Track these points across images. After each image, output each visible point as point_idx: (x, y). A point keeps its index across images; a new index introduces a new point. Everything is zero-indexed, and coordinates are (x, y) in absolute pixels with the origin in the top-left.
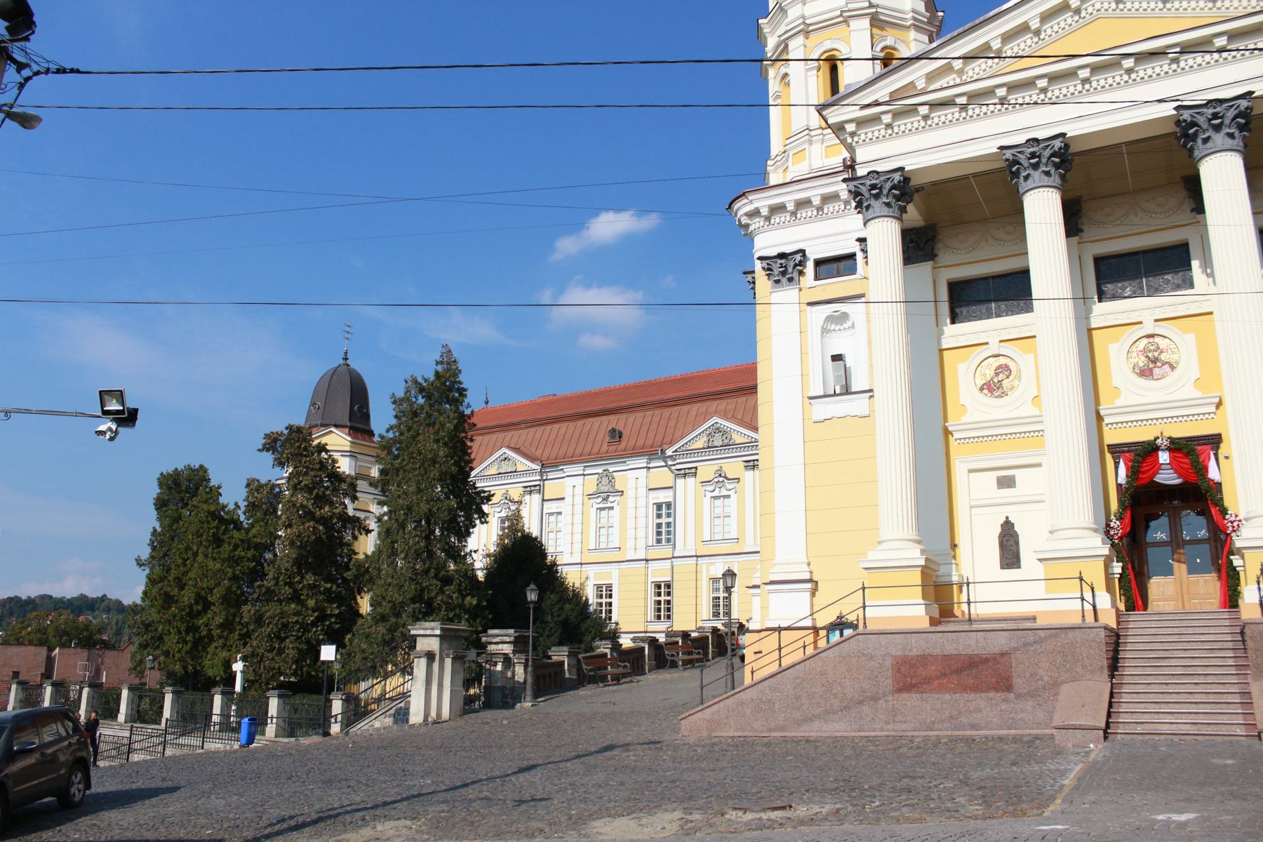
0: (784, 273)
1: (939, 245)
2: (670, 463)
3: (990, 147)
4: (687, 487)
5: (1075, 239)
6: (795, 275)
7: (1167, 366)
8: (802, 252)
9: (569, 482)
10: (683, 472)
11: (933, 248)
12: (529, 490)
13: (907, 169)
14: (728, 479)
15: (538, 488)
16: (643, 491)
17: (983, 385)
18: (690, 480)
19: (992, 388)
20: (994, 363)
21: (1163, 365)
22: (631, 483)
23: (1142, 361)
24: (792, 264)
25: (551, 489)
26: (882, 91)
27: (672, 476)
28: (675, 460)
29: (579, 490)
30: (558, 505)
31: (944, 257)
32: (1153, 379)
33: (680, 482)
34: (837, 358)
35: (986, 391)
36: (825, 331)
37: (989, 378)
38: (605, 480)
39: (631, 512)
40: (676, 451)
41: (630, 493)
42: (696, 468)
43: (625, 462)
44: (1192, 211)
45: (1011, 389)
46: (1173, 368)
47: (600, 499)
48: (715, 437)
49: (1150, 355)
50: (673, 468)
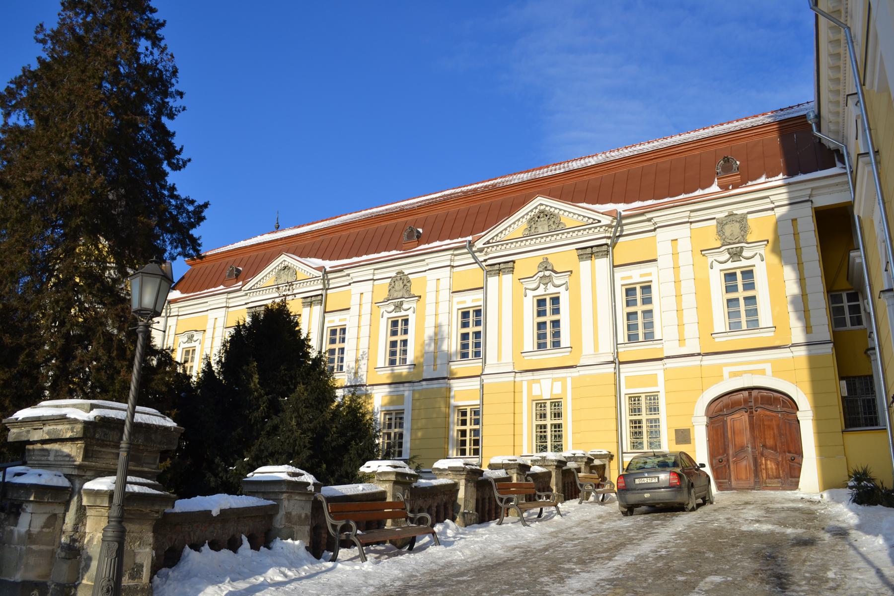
10: (497, 267)
14: (556, 272)
15: (319, 298)
16: (445, 294)
18: (507, 278)
22: (431, 286)
27: (482, 274)
28: (486, 254)
29: (367, 298)
33: (493, 281)
38: (399, 285)
40: (488, 242)
41: (430, 298)
42: (514, 262)
43: (423, 260)
48: (539, 223)
50: (484, 264)
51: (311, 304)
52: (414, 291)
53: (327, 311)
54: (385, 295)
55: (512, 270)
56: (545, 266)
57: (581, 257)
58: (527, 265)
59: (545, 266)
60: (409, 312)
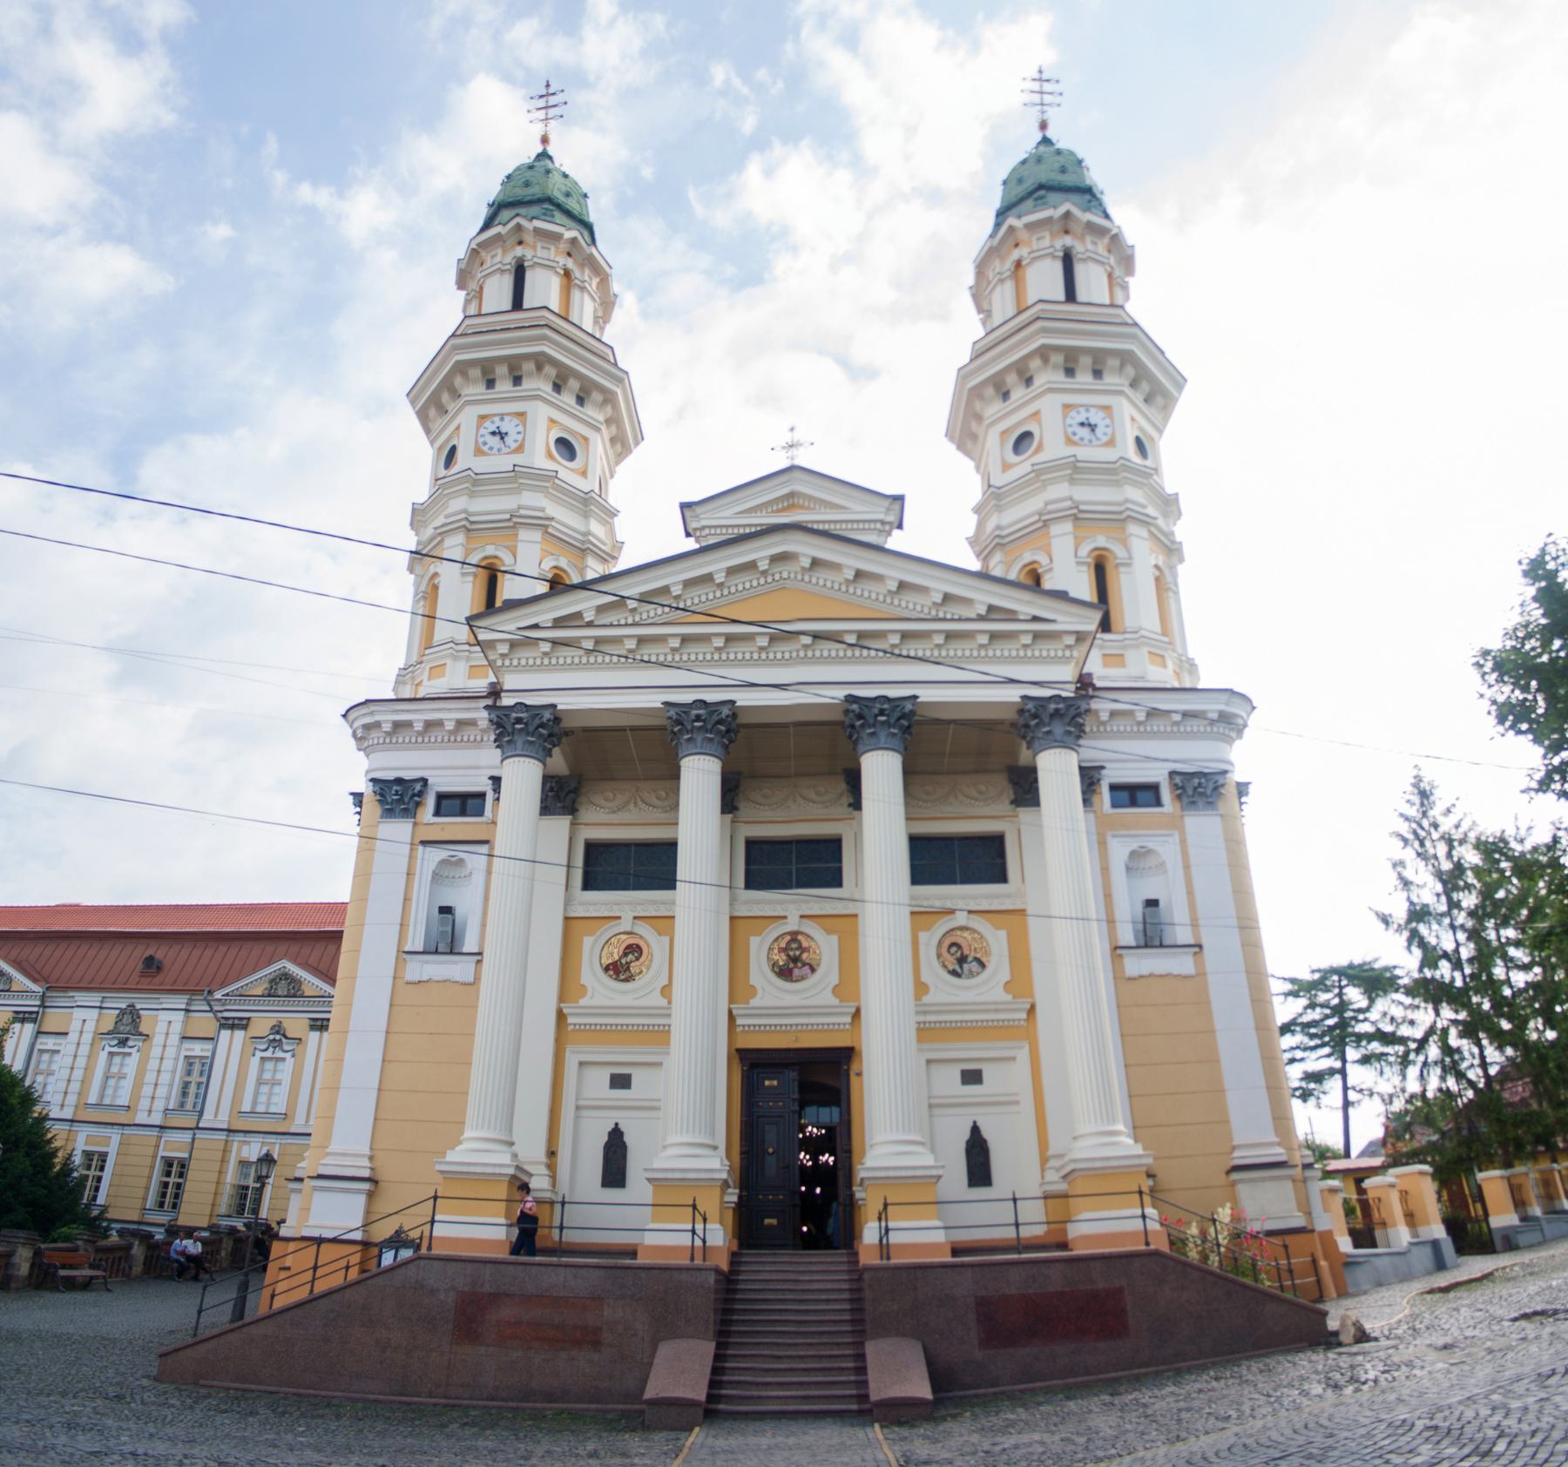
0: (401, 801)
1: (583, 799)
2: (216, 1008)
3: (654, 700)
4: (231, 1043)
5: (729, 817)
6: (411, 805)
7: (806, 969)
8: (424, 781)
9: (79, 1014)
10: (230, 1022)
11: (574, 802)
12: (22, 1017)
13: (559, 707)
14: (286, 1038)
16: (174, 1039)
18: (239, 1034)
19: (618, 970)
22: (161, 1027)
23: (781, 959)
24: (410, 793)
25: (52, 1020)
26: (546, 614)
29: (90, 1026)
30: (58, 1041)
31: (588, 814)
32: (792, 981)
33: (225, 1034)
34: (446, 910)
35: (611, 972)
36: (436, 876)
37: (617, 958)
38: (127, 1019)
39: (153, 1064)
40: (227, 995)
41: (158, 1040)
42: (249, 1019)
44: (850, 805)
45: (641, 972)
46: (813, 970)
47: (116, 1042)
49: (791, 953)
50: (219, 1015)
51: (23, 1021)
52: (143, 1028)
53: (43, 1030)
54: (111, 1027)
55: (245, 1027)
56: (278, 1029)
57: (313, 1028)
58: (262, 1024)
59: (278, 1029)
60: (133, 1051)
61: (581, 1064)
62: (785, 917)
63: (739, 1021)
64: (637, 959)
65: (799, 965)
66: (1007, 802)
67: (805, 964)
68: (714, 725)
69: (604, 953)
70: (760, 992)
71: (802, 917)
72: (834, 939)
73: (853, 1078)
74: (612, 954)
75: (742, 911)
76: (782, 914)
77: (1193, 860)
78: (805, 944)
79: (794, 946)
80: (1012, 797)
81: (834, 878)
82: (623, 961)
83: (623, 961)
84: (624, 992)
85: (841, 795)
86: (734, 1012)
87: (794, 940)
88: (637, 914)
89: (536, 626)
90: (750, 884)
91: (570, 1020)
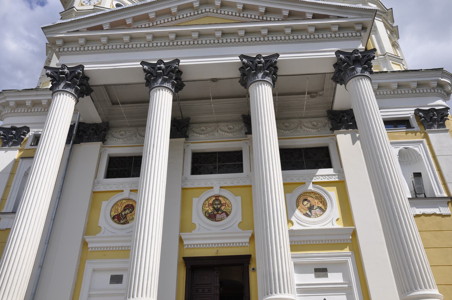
7: (224, 214)
11: (105, 136)
13: (85, 69)
17: (115, 216)
20: (125, 203)
21: (222, 213)
32: (216, 221)
35: (116, 220)
37: (120, 212)
44: (246, 133)
46: (227, 215)
49: (215, 206)
61: (94, 270)
62: (212, 188)
63: (185, 243)
64: (131, 212)
65: (220, 212)
66: (329, 129)
67: (223, 212)
68: (169, 73)
69: (113, 210)
70: (197, 226)
71: (221, 187)
72: (239, 198)
73: (251, 274)
74: (117, 210)
75: (189, 185)
76: (211, 186)
77: (437, 153)
78: (223, 202)
79: (217, 202)
80: (331, 126)
81: (239, 169)
82: (123, 213)
83: (123, 213)
84: (122, 229)
85: (242, 129)
86: (183, 237)
87: (216, 200)
88: (132, 189)
89: (78, 31)
90: (195, 171)
91: (90, 245)
